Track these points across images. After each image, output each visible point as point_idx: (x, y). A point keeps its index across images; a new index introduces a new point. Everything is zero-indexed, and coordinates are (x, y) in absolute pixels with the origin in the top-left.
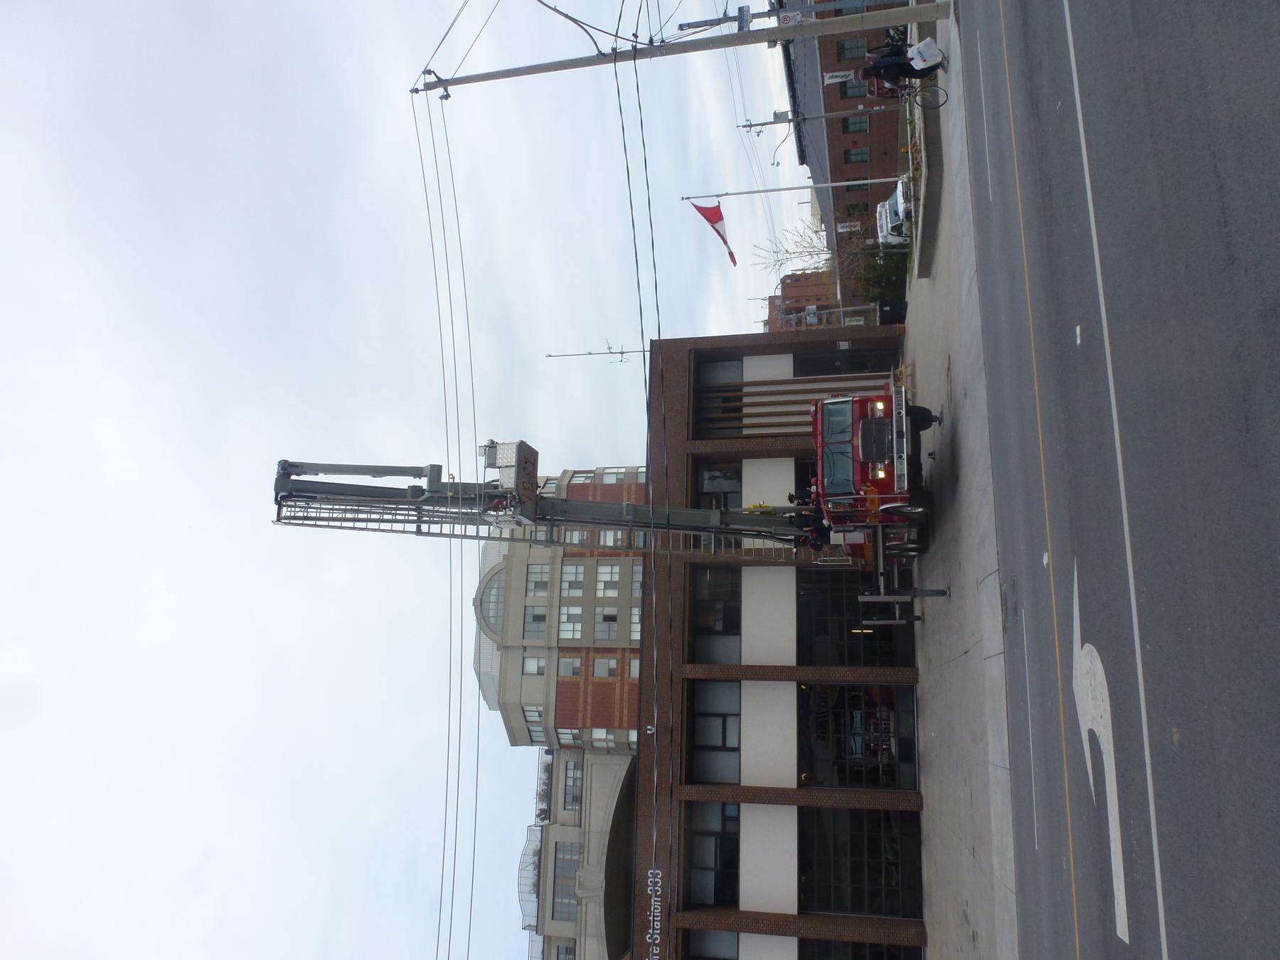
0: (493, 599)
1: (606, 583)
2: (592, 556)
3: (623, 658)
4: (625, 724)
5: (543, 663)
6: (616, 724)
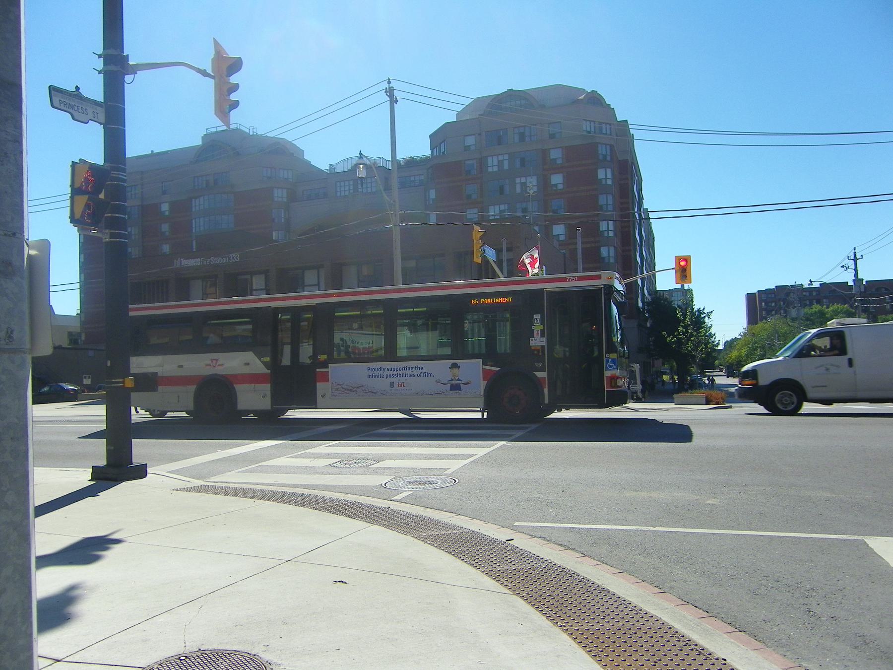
1: (526, 183)
5: (473, 148)
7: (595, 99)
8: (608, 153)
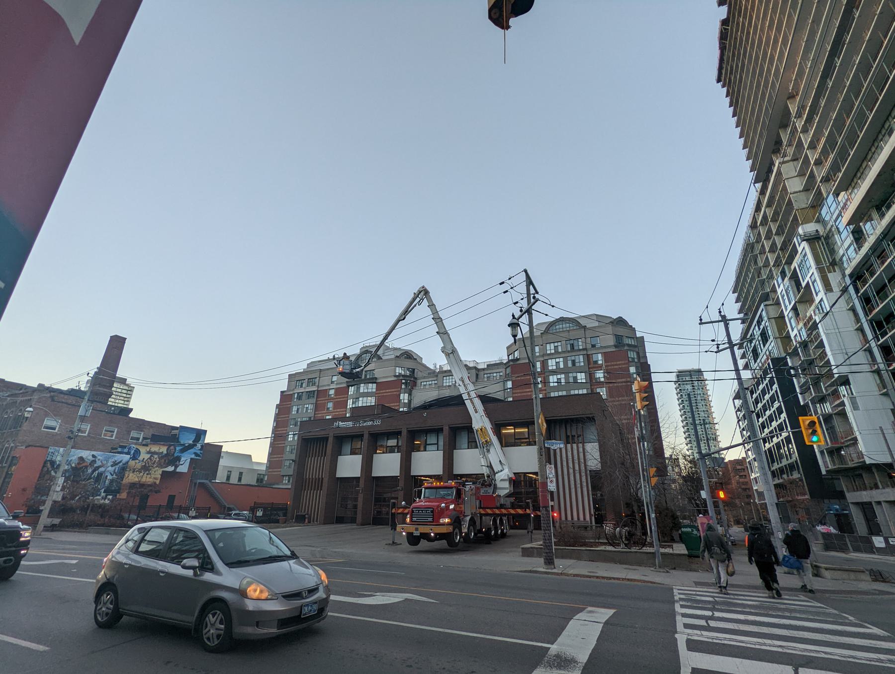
0: (564, 326)
1: (576, 377)
2: (589, 368)
3: (544, 390)
4: (514, 395)
6: (514, 391)
7: (620, 322)
8: (635, 357)
